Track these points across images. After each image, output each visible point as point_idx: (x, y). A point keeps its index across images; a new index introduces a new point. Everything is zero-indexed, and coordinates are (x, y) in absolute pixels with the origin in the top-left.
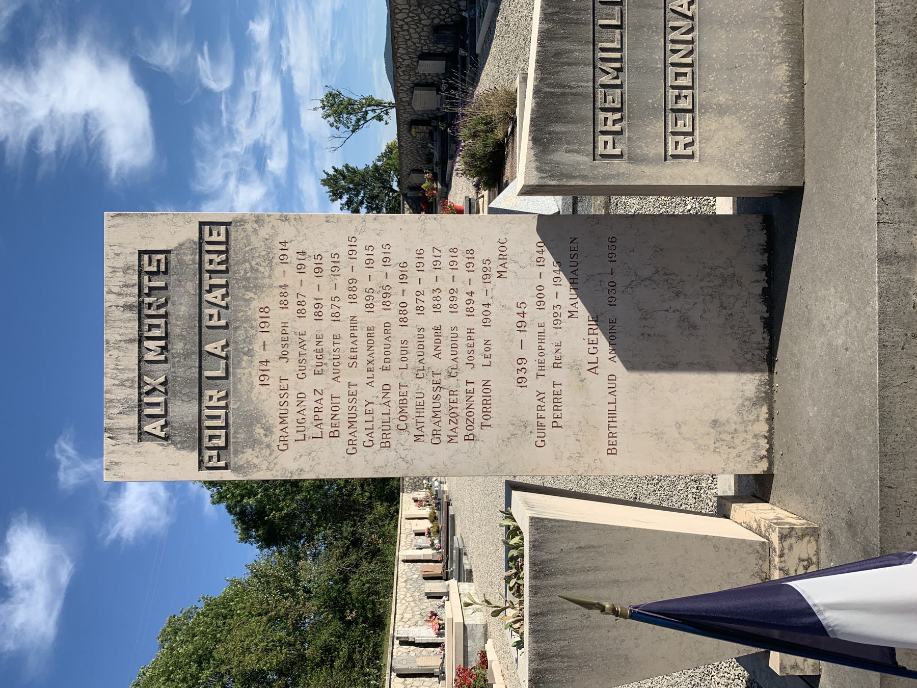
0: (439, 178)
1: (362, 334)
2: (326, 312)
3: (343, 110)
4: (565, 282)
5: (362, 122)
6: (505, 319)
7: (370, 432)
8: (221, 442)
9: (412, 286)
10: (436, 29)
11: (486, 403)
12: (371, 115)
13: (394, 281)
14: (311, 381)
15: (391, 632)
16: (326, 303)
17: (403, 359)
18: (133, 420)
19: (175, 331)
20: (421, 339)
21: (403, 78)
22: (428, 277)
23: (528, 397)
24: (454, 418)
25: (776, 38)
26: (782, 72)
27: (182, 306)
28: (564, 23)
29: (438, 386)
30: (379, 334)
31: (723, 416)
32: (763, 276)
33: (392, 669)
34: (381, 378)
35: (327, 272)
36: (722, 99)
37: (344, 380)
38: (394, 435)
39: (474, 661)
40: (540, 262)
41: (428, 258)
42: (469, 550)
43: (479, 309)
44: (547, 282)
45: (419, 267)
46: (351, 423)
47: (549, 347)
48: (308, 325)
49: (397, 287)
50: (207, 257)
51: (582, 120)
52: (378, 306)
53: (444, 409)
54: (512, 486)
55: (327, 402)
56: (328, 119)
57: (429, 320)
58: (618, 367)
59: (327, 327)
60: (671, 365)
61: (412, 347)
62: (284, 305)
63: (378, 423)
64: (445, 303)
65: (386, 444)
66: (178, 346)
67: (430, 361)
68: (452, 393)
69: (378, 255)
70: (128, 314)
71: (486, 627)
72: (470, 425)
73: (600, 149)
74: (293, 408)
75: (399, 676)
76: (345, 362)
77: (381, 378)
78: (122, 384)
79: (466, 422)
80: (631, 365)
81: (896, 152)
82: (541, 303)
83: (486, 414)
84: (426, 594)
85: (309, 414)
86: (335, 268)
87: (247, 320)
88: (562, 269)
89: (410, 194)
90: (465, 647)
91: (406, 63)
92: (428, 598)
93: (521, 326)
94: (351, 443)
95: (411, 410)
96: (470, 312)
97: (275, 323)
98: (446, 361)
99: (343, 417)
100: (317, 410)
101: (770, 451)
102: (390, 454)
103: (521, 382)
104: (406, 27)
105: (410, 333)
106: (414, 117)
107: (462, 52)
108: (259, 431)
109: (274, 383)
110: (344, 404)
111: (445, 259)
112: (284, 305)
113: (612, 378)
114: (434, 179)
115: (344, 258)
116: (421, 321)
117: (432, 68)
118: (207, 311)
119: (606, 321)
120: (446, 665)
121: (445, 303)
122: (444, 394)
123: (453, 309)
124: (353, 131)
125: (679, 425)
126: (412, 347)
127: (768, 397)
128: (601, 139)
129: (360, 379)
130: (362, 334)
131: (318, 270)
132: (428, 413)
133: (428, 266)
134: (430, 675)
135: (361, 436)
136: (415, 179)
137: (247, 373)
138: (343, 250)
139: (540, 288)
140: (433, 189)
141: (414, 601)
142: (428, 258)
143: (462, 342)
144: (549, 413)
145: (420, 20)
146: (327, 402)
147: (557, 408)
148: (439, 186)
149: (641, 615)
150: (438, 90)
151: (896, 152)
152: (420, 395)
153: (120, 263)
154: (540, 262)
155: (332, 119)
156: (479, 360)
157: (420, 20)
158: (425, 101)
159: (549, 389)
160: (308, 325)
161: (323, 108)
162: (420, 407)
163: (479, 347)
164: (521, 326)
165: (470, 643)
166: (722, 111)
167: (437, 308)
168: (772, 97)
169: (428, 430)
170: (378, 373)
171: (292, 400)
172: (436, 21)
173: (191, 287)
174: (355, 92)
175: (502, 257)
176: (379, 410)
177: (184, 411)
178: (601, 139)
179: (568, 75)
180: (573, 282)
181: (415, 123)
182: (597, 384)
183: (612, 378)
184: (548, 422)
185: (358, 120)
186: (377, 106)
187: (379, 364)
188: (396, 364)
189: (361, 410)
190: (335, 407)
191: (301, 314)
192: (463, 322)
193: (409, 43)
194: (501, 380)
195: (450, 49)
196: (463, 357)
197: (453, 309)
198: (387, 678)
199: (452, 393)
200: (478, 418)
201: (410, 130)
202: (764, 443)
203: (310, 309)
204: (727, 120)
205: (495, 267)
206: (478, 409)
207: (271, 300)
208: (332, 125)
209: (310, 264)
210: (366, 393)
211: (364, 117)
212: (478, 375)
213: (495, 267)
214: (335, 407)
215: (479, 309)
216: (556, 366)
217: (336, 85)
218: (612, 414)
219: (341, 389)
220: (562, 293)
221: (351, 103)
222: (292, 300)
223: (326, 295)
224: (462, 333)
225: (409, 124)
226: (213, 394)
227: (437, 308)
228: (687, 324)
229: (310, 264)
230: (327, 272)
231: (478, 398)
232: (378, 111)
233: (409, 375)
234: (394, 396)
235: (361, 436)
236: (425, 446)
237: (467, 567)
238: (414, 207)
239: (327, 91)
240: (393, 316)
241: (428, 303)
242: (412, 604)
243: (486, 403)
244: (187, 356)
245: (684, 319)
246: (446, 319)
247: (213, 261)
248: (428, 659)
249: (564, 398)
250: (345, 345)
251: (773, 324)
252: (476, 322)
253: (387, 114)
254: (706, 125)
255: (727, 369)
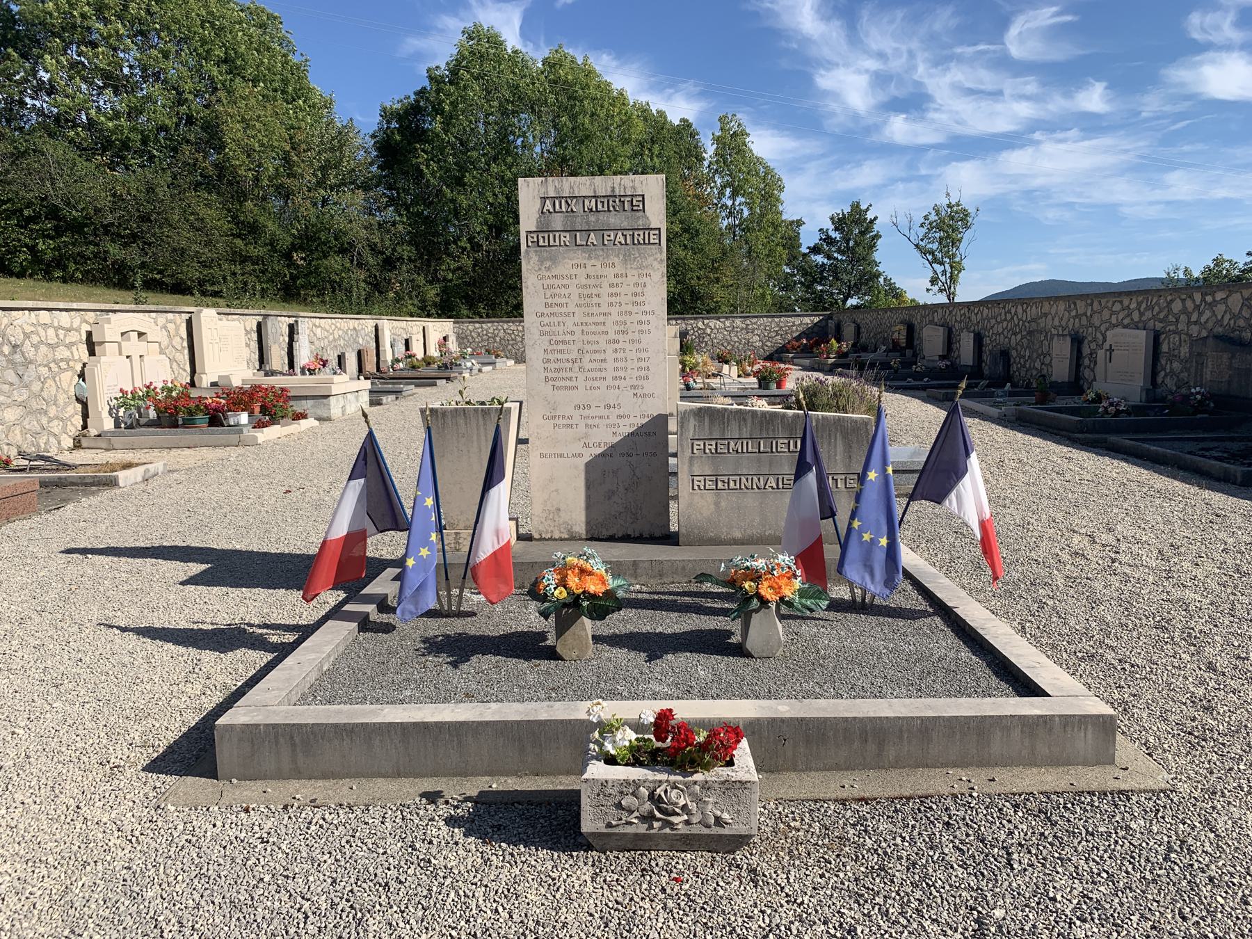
0: (842, 361)
1: (601, 319)
2: (613, 299)
3: (946, 233)
4: (632, 430)
5: (930, 257)
6: (611, 397)
7: (549, 325)
8: (541, 243)
9: (628, 346)
10: (1005, 354)
11: (566, 388)
12: (939, 269)
13: (630, 336)
14: (575, 292)
15: (302, 314)
16: (618, 299)
17: (589, 342)
18: (552, 194)
19: (601, 216)
20: (600, 352)
21: (958, 314)
22: (633, 355)
23: (569, 410)
24: (557, 370)
25: (756, 532)
26: (738, 534)
27: (614, 220)
28: (761, 423)
29: (574, 361)
30: (601, 328)
31: (562, 514)
32: (637, 534)
33: (265, 316)
34: (578, 330)
35: (634, 299)
36: (723, 504)
37: (576, 310)
38: (548, 338)
39: (298, 407)
40: (642, 416)
41: (644, 355)
42: (402, 402)
43: (616, 383)
44: (632, 420)
45: (639, 350)
46: (553, 314)
47: (597, 421)
48: (606, 289)
49: (627, 338)
50: (641, 233)
51: (711, 433)
52: (617, 328)
53: (562, 365)
54: (521, 403)
55: (564, 300)
56: (934, 213)
57: (610, 356)
58: (587, 458)
59: (605, 299)
60: (589, 486)
61: (595, 347)
62: (616, 276)
63: (553, 329)
64: (619, 365)
65: (542, 333)
66: (592, 218)
67: (588, 357)
68: (571, 369)
69: (645, 327)
70: (609, 190)
71: (328, 419)
72: (554, 379)
73: (696, 442)
74: (560, 282)
75: (259, 325)
76: (586, 310)
77: (578, 330)
78: (571, 187)
79: (556, 377)
80: (588, 465)
81: (684, 568)
82: (620, 417)
83: (560, 388)
84: (343, 354)
85: (558, 291)
86: (638, 304)
87: (608, 256)
88: (639, 428)
89: (831, 324)
90: (306, 398)
91: (973, 317)
92: (339, 357)
93: (608, 406)
94: (543, 314)
95: (561, 347)
96: (614, 378)
97: (606, 271)
98: (588, 366)
99: (556, 310)
100: (560, 296)
101: (545, 539)
102: (537, 336)
103: (578, 407)
104: (1009, 317)
105: (603, 345)
106: (917, 328)
107: (983, 383)
108: (548, 264)
109: (574, 271)
110: (563, 310)
111: (643, 364)
112: (616, 276)
113: (581, 455)
114: (841, 355)
115: (643, 308)
116: (609, 351)
117: (966, 351)
118: (612, 234)
119: (611, 451)
120: (280, 377)
121: (619, 365)
122: (570, 365)
123: (616, 369)
124: (917, 246)
125: (557, 491)
126: (595, 347)
127: (573, 538)
128: (701, 443)
129: (577, 319)
130: (601, 319)
131: (635, 294)
132: (559, 356)
133: (639, 355)
134: (262, 360)
135: (546, 320)
136: (849, 330)
137: (579, 257)
138: (647, 308)
139: (629, 416)
140: (828, 354)
141: (335, 340)
142: (644, 355)
143: (598, 374)
144: (561, 422)
145: (1016, 334)
146: (564, 300)
147: (564, 426)
148: (830, 361)
149: (498, 426)
150: (943, 357)
151: (684, 568)
152: (569, 352)
153: (637, 184)
154: (642, 416)
155: (933, 217)
156: (589, 384)
157: (1016, 334)
158: (932, 341)
159: (574, 422)
160: (606, 289)
161: (949, 206)
162: (562, 352)
163: (596, 384)
164: (608, 406)
165: (310, 403)
166: (717, 504)
167: (616, 360)
168: (725, 530)
169: (550, 356)
170: (581, 328)
171: (565, 282)
172: (1014, 353)
173: (625, 224)
174: (970, 246)
175: (645, 395)
176: (560, 329)
177: (557, 222)
178: (701, 443)
179: (734, 424)
180: (632, 434)
181: (910, 329)
182: (578, 447)
183: (581, 455)
184: (556, 421)
185: (932, 252)
186: (951, 277)
187: (585, 328)
188: (585, 338)
189: (560, 319)
190: (562, 305)
191: (612, 285)
192: (609, 374)
193: (993, 321)
194: (579, 396)
195: (986, 371)
196: (590, 375)
197: (616, 369)
198: (256, 311)
199: (571, 369)
200: (558, 384)
201: (901, 323)
202: (548, 536)
203: (614, 290)
204: (712, 507)
205: (639, 391)
206: (562, 383)
207: (619, 269)
208: (926, 218)
209: (639, 290)
210: (569, 322)
211: (935, 260)
212: (581, 383)
213: (639, 391)
214: (562, 305)
215: (616, 383)
216: (587, 425)
217: (976, 221)
218: (561, 456)
219: (571, 308)
220: (626, 428)
221: (955, 243)
222: (619, 280)
223: (622, 299)
224: (603, 374)
225: (914, 318)
226: (567, 238)
227: (616, 360)
228: (610, 494)
229: (639, 290)
230: (634, 299)
231: (568, 383)
232: (943, 279)
233: (580, 345)
234: (568, 337)
235: (546, 320)
236: (542, 355)
237: (384, 399)
238: (816, 329)
239: (971, 210)
240: (611, 336)
241: (619, 355)
242: (331, 338)
243: (566, 388)
244: (587, 223)
245: (613, 493)
246: (610, 365)
247: (639, 237)
248: (278, 359)
249: (569, 430)
250: (595, 310)
251: (611, 539)
252: (609, 382)
253: (941, 291)
254: (710, 497)
255: (587, 516)
